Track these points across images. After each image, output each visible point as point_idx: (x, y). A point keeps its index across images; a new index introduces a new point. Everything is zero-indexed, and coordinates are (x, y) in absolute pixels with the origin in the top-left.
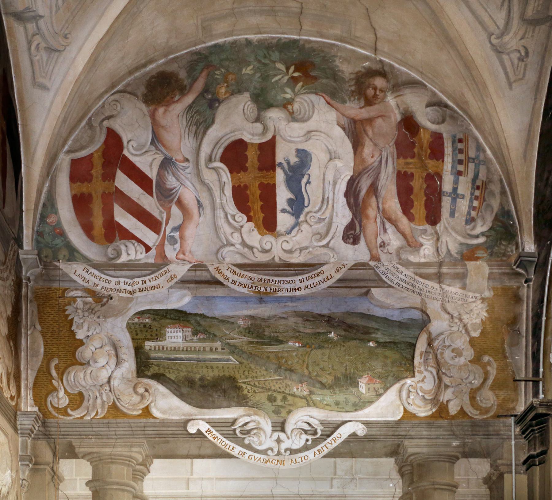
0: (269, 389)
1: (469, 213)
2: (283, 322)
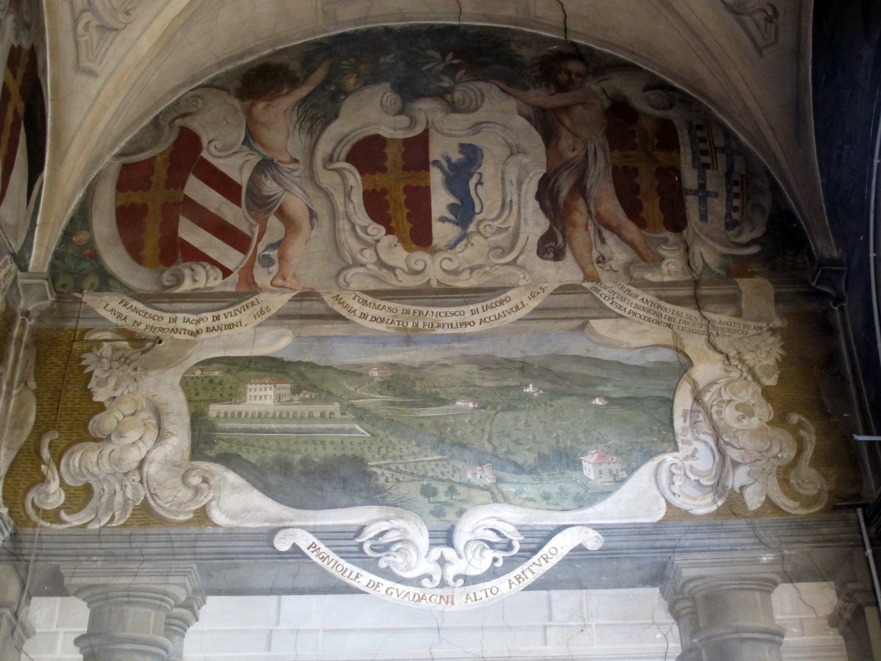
0: (424, 476)
1: (728, 215)
2: (447, 371)
